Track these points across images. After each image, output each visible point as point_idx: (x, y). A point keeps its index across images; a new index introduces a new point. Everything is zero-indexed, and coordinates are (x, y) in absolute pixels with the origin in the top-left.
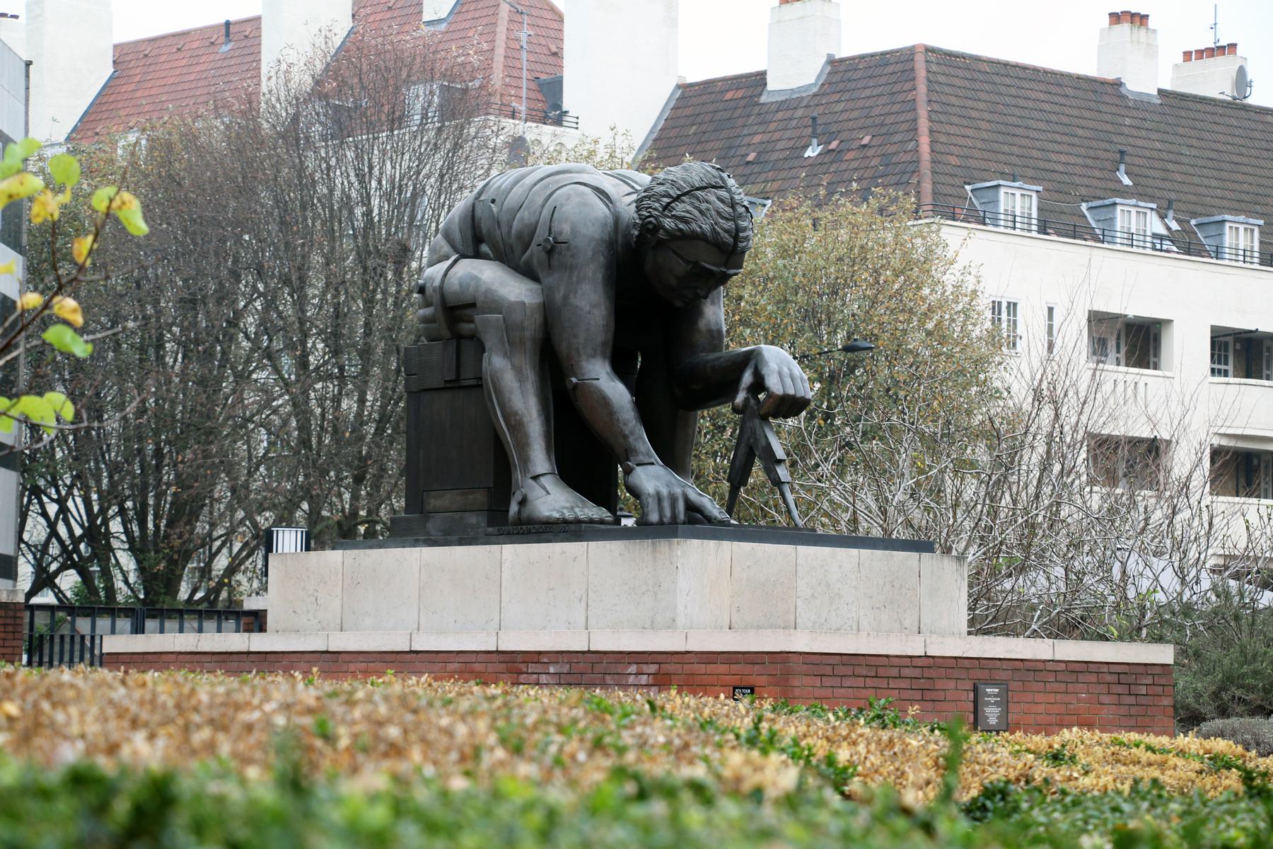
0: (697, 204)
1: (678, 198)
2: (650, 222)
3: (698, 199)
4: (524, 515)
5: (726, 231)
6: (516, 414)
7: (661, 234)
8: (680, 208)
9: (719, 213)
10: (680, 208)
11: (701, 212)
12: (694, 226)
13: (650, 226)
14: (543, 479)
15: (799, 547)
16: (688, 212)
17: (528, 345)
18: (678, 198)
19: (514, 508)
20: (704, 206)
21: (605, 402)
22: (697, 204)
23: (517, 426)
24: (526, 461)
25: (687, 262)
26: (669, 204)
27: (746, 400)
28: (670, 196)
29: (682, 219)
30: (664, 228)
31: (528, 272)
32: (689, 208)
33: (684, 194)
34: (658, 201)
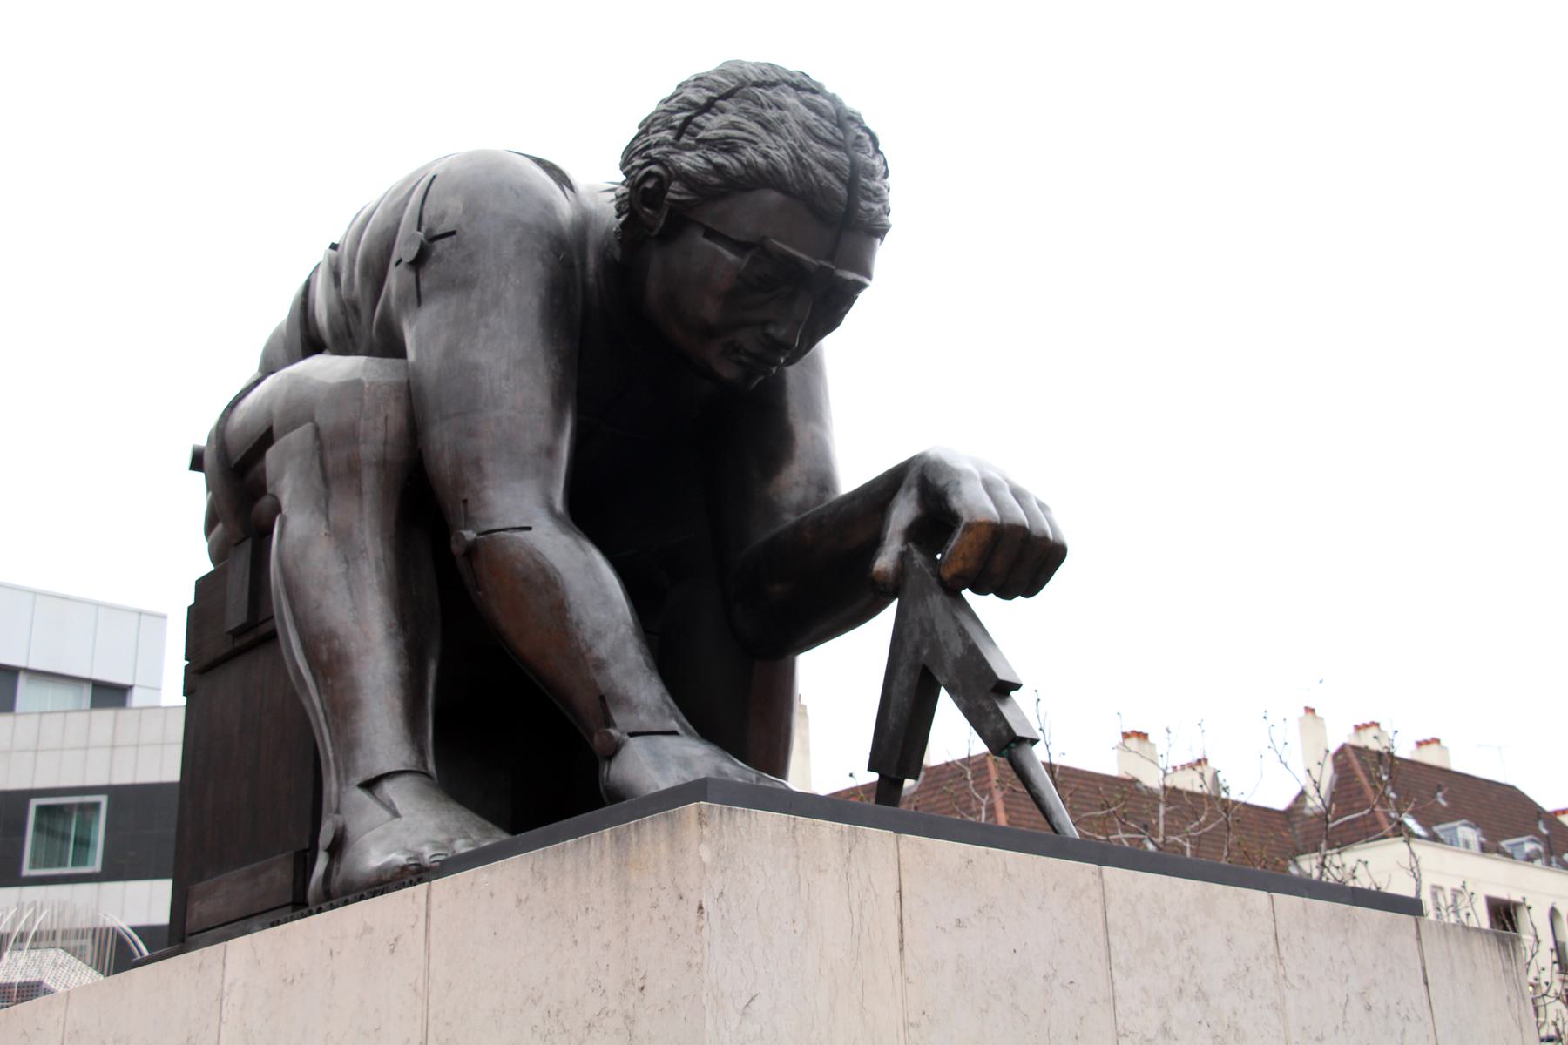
0: (754, 109)
1: (709, 107)
2: (650, 175)
3: (757, 102)
5: (829, 166)
6: (331, 635)
7: (675, 192)
9: (808, 129)
11: (766, 125)
12: (749, 153)
13: (649, 185)
14: (389, 789)
15: (1106, 869)
16: (733, 125)
17: (369, 479)
18: (709, 107)
20: (771, 114)
21: (544, 585)
22: (754, 109)
23: (330, 663)
24: (348, 746)
25: (740, 247)
26: (688, 120)
27: (903, 557)
32: (734, 118)
33: (724, 97)
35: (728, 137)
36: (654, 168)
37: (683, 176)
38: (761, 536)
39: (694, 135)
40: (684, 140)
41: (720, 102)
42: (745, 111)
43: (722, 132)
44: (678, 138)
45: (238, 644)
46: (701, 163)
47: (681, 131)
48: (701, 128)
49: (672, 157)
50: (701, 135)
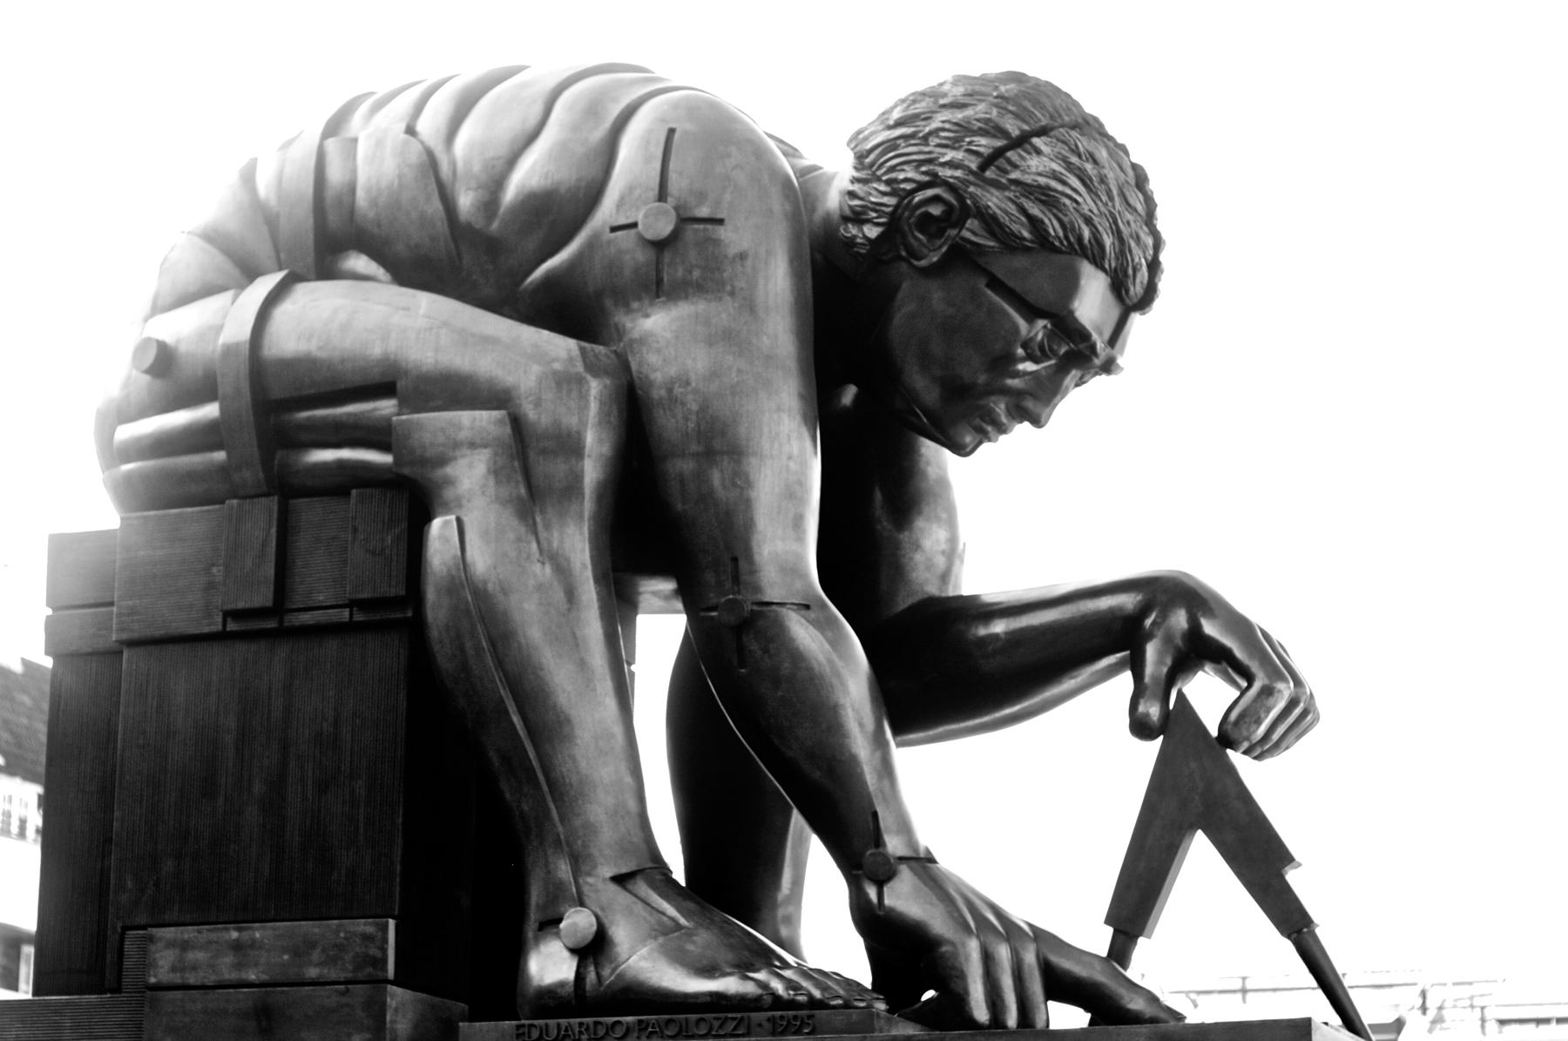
1: (1022, 141)
2: (936, 199)
8: (1038, 165)
10: (1038, 165)
13: (936, 210)
18: (1022, 141)
19: (550, 965)
26: (998, 153)
28: (1000, 132)
29: (1047, 198)
31: (571, 310)
32: (1055, 166)
34: (954, 144)
35: (1049, 188)
37: (991, 223)
38: (903, 603)
39: (1006, 172)
40: (990, 174)
41: (1036, 141)
42: (1065, 160)
43: (1042, 180)
44: (983, 167)
45: (232, 626)
46: (1012, 209)
47: (988, 161)
48: (1016, 167)
49: (972, 189)
50: (1014, 175)
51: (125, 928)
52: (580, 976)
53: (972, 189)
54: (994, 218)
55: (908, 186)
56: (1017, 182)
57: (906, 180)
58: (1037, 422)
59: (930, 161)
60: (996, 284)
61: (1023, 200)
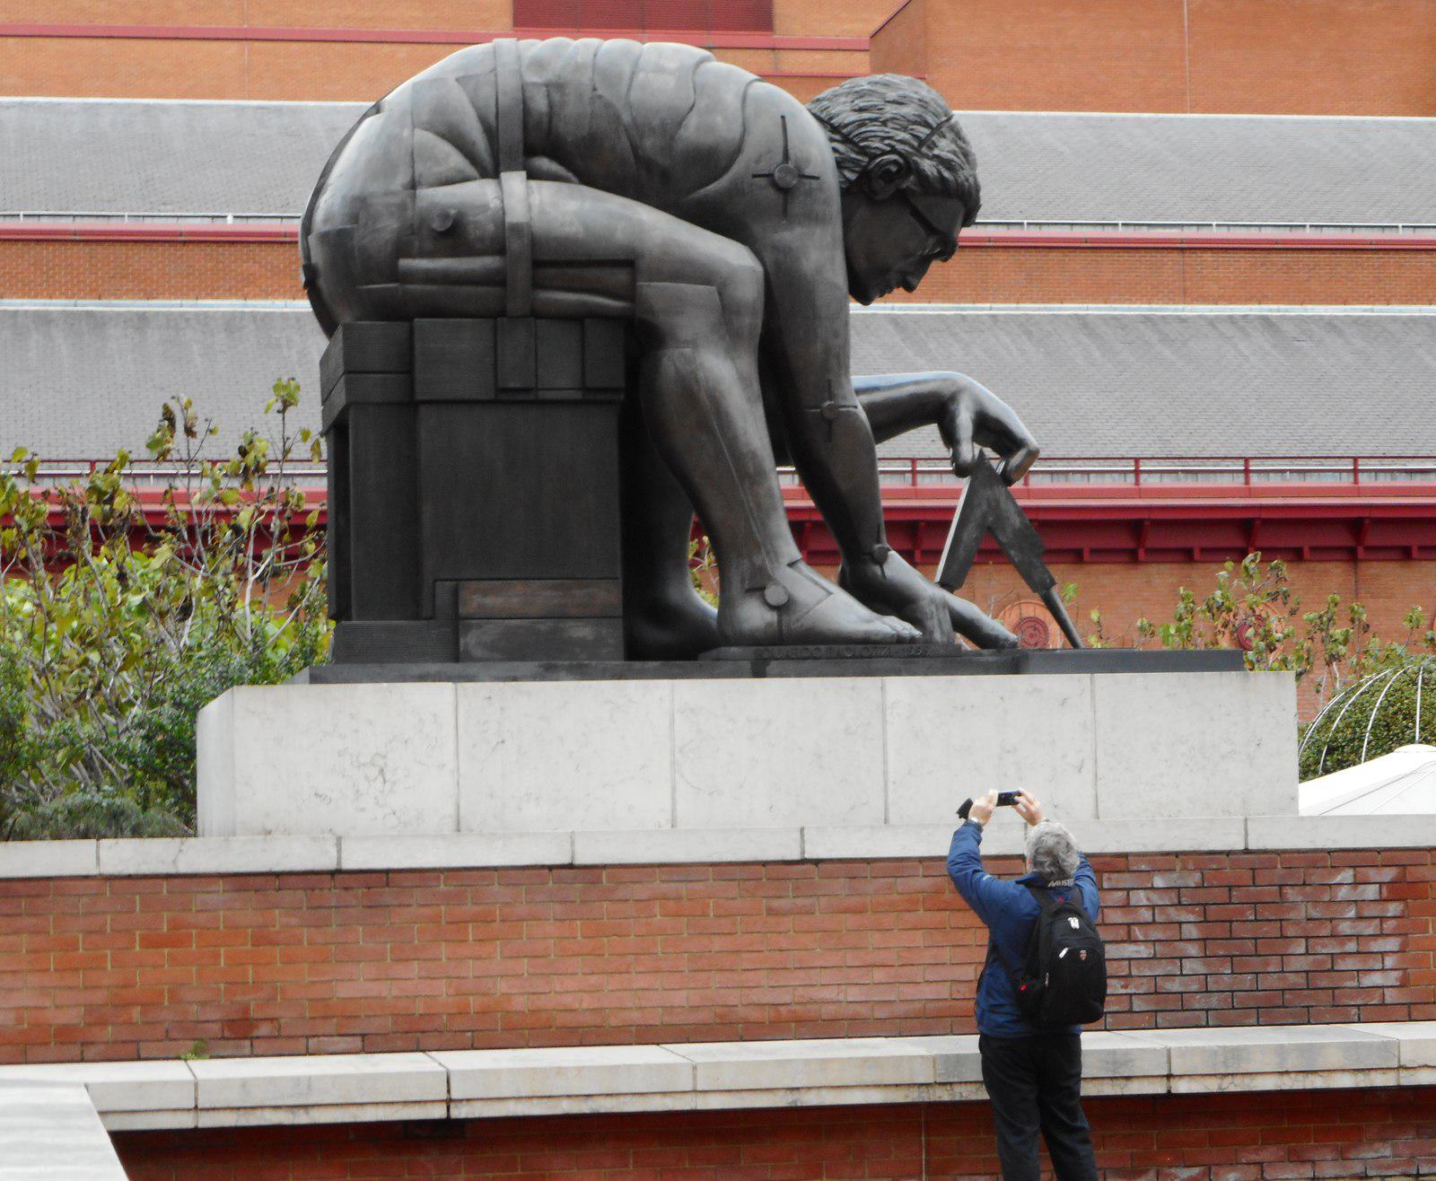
2: (895, 162)
4: (796, 623)
8: (944, 147)
13: (894, 169)
28: (927, 125)
29: (948, 164)
30: (921, 175)
34: (905, 129)
36: (901, 161)
43: (951, 156)
45: (504, 397)
50: (936, 152)
51: (435, 581)
52: (780, 622)
53: (915, 158)
54: (927, 177)
55: (879, 152)
56: (937, 157)
57: (877, 148)
58: (910, 288)
59: (889, 138)
60: (916, 214)
61: (940, 167)
